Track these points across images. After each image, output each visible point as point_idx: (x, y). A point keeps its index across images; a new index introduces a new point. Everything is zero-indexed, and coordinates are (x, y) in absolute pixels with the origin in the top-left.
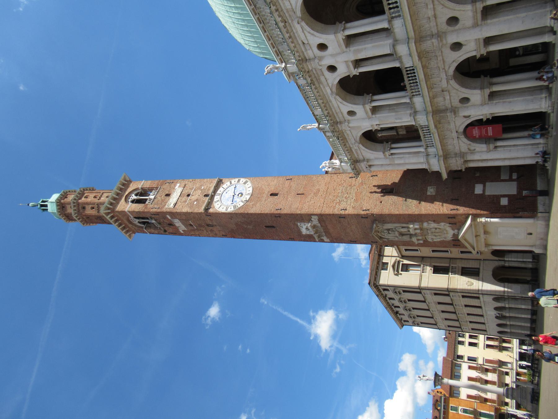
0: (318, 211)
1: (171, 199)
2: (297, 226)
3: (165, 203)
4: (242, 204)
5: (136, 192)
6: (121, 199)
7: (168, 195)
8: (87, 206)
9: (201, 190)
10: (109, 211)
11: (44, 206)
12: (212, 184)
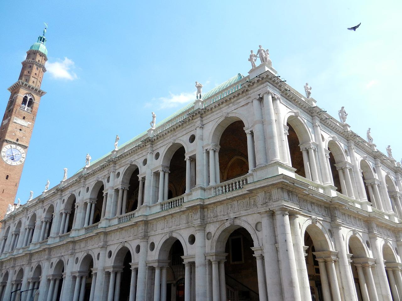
1: (20, 120)
4: (5, 160)
5: (33, 99)
7: (24, 118)
10: (21, 84)
11: (42, 39)
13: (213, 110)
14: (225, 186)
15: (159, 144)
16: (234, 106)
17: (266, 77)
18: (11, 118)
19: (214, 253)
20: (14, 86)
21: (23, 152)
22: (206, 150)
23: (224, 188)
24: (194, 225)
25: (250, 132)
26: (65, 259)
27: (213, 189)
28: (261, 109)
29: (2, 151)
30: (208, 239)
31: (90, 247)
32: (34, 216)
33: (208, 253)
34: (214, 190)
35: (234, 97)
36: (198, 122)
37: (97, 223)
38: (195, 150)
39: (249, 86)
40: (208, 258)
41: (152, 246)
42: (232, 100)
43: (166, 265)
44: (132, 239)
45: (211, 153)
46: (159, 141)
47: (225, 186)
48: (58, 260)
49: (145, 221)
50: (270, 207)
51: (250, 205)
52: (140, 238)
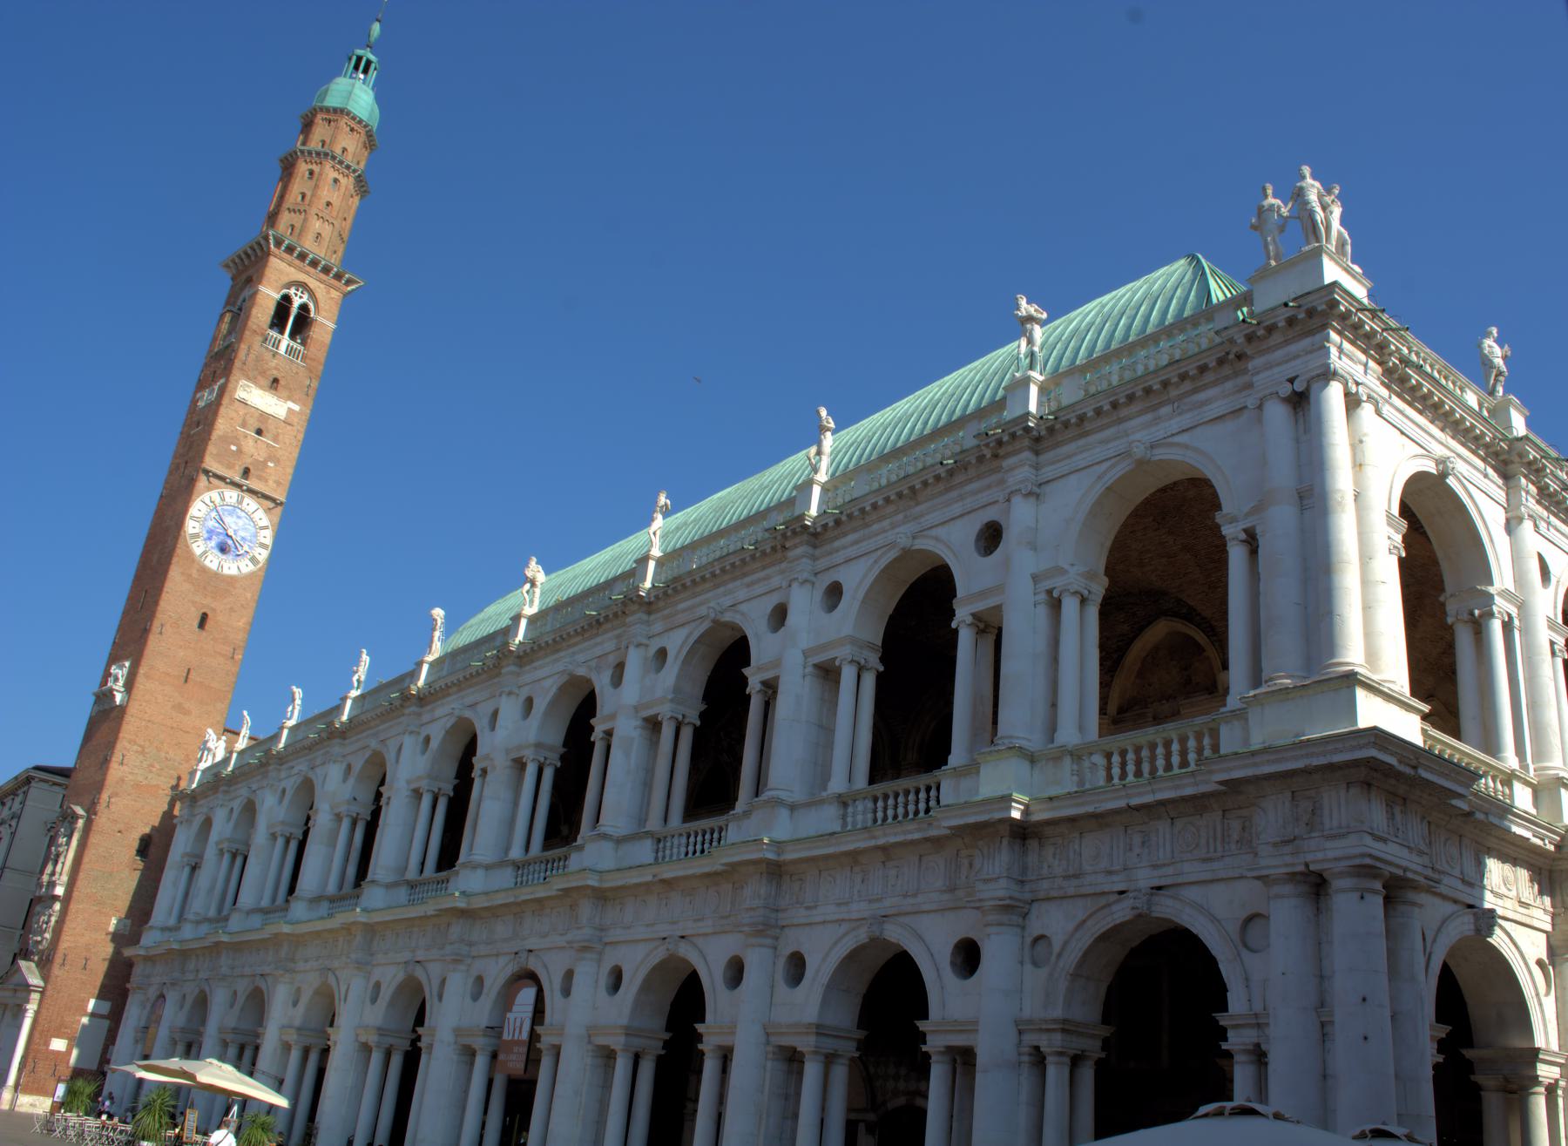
0: (133, 710)
2: (126, 658)
3: (256, 378)
6: (301, 270)
8: (312, 183)
9: (264, 463)
12: (275, 485)
13: (1088, 426)
14: (1123, 753)
15: (845, 547)
16: (1180, 414)
17: (1324, 307)
18: (227, 381)
19: (1055, 1021)
20: (246, 253)
21: (265, 522)
22: (1050, 592)
23: (1116, 759)
24: (981, 900)
25: (1243, 536)
26: (429, 978)
27: (1067, 761)
28: (1297, 441)
29: (188, 517)
30: (1035, 964)
31: (532, 943)
32: (307, 788)
33: (1030, 1021)
34: (1075, 767)
35: (1183, 377)
36: (1020, 469)
37: (565, 849)
38: (999, 589)
39: (1250, 338)
40: (1030, 1039)
41: (797, 967)
42: (1173, 393)
43: (849, 1049)
44: (709, 930)
45: (1070, 606)
46: (845, 534)
47: (1123, 753)
48: (401, 976)
49: (769, 863)
50: (1309, 857)
51: (1223, 840)
52: (746, 929)
